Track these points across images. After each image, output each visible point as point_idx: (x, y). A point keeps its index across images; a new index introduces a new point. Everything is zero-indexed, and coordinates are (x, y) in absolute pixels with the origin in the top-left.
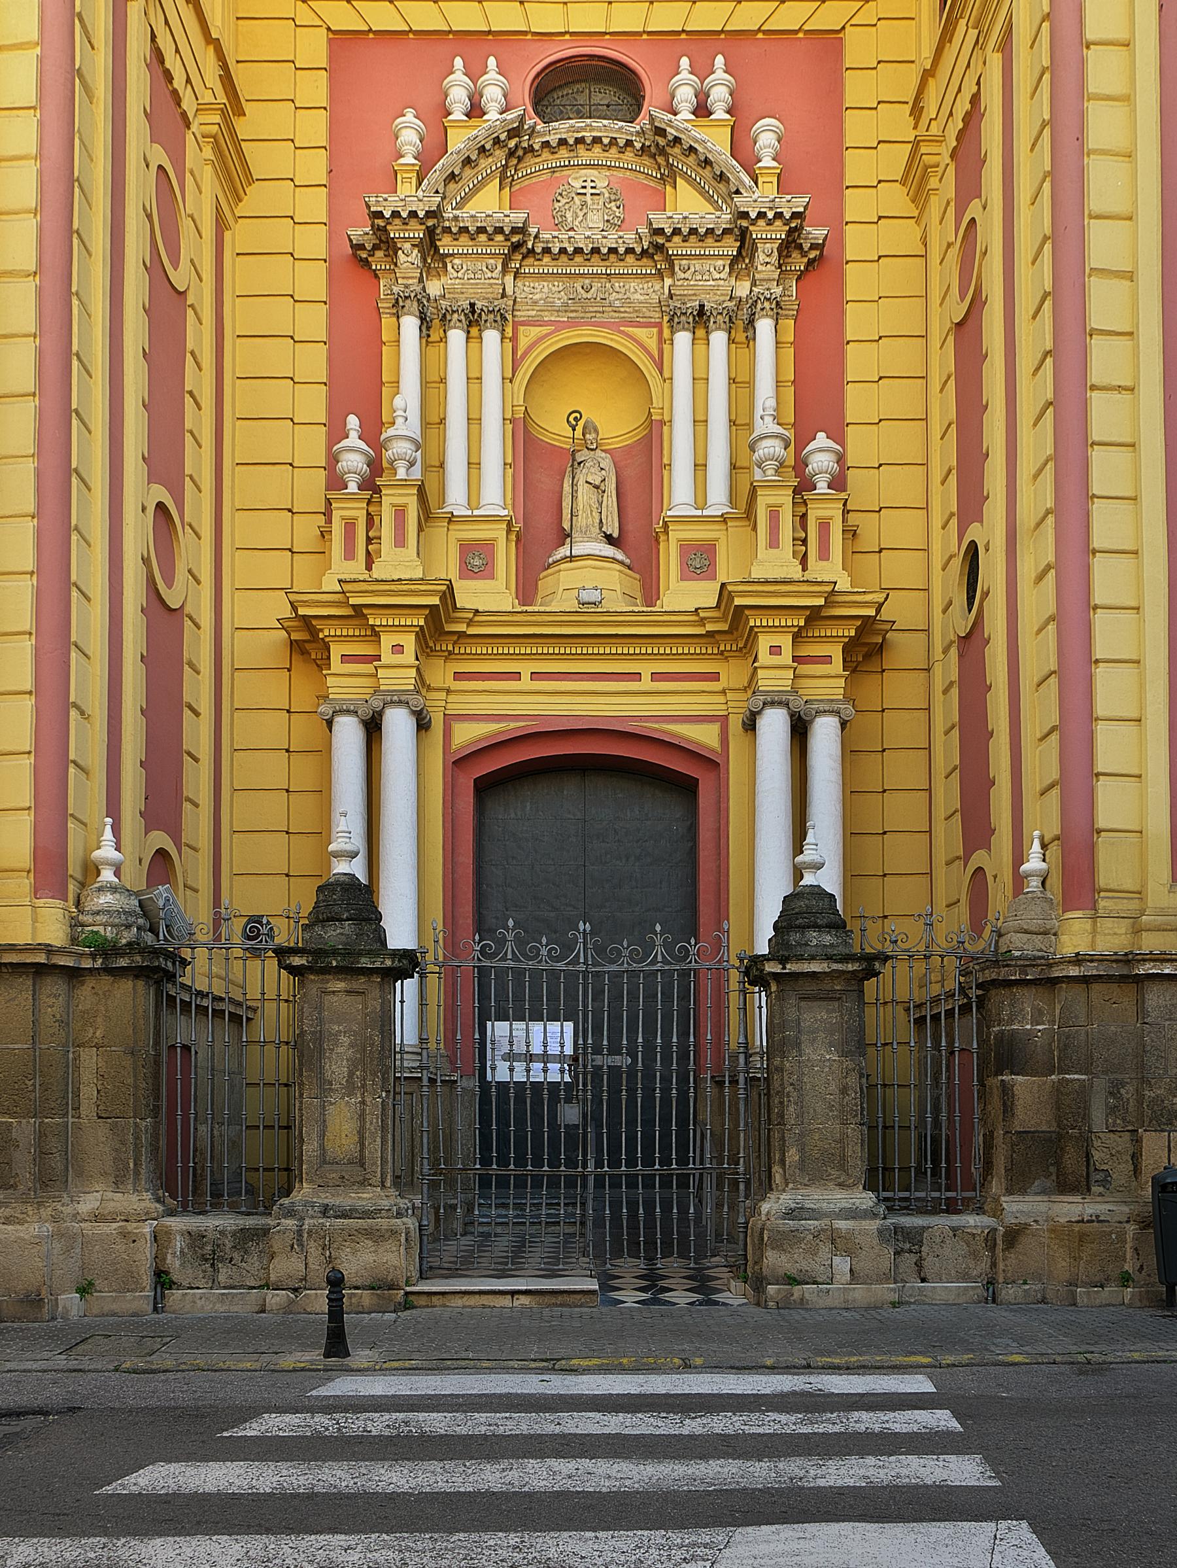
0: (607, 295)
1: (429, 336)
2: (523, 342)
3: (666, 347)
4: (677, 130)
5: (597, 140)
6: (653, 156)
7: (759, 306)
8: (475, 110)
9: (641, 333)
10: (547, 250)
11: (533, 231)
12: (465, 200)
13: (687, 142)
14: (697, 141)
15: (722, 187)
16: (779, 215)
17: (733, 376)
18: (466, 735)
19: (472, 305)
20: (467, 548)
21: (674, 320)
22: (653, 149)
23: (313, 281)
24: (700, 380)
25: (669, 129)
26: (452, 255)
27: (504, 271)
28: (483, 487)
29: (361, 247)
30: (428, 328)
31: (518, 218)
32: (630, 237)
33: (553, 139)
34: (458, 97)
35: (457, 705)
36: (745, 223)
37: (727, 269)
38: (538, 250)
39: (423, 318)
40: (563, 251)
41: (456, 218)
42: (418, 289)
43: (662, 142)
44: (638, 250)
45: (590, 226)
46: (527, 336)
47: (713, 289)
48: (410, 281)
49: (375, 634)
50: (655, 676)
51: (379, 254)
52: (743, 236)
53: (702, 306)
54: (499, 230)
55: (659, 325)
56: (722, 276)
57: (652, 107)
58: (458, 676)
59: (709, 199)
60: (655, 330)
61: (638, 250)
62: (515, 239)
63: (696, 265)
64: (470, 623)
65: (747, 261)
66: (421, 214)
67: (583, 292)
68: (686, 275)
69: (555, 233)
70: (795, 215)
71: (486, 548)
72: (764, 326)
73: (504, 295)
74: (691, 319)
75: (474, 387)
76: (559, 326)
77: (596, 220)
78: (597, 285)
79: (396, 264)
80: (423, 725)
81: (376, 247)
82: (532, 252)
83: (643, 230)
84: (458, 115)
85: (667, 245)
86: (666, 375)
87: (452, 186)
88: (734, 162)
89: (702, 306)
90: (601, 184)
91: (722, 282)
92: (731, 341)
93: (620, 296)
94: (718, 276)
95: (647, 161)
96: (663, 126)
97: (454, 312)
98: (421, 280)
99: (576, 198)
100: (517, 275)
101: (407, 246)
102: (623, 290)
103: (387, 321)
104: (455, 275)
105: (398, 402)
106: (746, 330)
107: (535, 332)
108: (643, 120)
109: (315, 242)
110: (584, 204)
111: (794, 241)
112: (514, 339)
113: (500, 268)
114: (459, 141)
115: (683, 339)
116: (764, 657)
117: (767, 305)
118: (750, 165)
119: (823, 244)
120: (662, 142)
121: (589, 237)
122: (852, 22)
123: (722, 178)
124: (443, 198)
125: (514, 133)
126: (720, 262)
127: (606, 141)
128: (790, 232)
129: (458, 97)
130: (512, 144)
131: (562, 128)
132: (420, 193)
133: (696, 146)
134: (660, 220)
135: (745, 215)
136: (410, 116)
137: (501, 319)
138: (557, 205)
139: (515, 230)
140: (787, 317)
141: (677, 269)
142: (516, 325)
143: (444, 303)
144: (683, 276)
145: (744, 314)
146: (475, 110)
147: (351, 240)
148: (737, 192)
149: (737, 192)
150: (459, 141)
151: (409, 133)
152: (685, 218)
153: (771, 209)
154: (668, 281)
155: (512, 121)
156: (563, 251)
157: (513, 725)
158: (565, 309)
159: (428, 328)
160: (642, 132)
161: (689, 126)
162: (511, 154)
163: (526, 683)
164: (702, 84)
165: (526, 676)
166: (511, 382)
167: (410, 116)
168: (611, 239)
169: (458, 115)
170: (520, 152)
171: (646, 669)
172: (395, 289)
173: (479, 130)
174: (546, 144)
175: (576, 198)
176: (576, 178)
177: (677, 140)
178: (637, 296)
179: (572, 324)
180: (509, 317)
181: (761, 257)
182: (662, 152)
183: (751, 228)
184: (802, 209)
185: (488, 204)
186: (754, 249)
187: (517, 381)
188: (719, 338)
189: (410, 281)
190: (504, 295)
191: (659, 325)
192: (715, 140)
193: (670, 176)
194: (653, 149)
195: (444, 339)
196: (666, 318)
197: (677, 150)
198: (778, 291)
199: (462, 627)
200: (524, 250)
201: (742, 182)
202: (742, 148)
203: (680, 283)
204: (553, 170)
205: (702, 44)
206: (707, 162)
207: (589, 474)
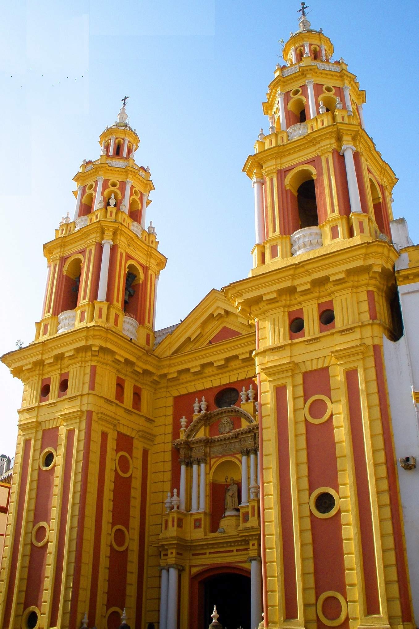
2: (212, 463)
18: (194, 570)
20: (196, 521)
23: (168, 456)
28: (201, 503)
33: (216, 413)
34: (196, 408)
35: (194, 562)
46: (213, 461)
49: (167, 550)
50: (237, 551)
58: (193, 555)
64: (191, 543)
71: (200, 520)
76: (220, 457)
77: (227, 430)
80: (181, 571)
84: (196, 413)
90: (229, 420)
100: (210, 447)
109: (169, 447)
115: (244, 458)
116: (251, 546)
129: (196, 408)
142: (211, 459)
146: (200, 410)
157: (204, 567)
163: (208, 555)
165: (208, 554)
169: (196, 413)
171: (234, 549)
174: (215, 415)
199: (190, 544)
207: (230, 493)
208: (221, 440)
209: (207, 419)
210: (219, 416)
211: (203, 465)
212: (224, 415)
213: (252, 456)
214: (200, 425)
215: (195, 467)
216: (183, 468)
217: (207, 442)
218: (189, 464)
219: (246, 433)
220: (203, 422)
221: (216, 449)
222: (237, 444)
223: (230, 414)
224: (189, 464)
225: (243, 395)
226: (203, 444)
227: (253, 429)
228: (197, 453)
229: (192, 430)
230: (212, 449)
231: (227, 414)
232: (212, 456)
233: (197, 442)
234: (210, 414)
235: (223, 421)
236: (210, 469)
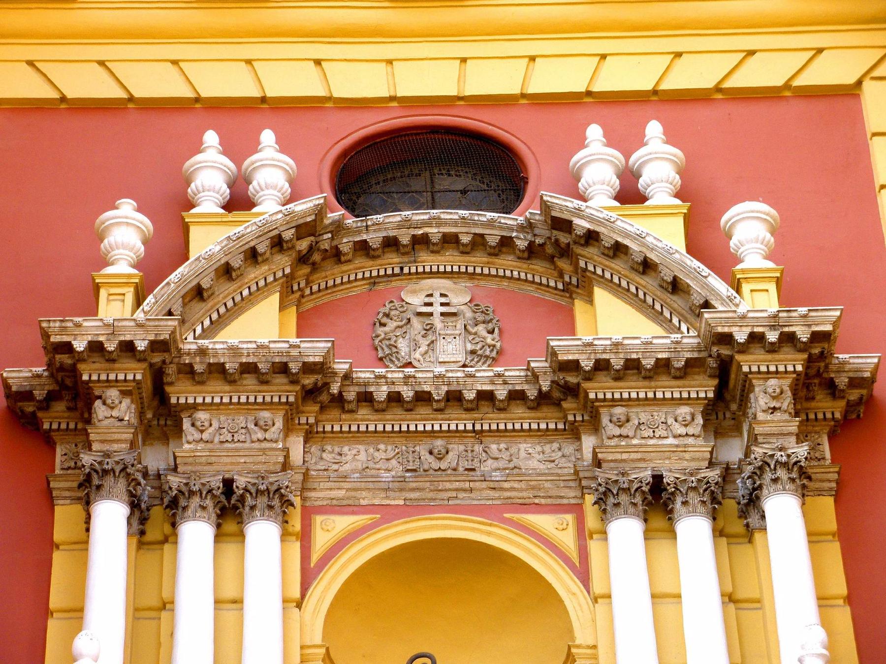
0: (476, 464)
1: (142, 533)
2: (322, 540)
3: (594, 546)
4: (591, 219)
5: (450, 240)
6: (551, 259)
7: (768, 476)
8: (239, 201)
9: (545, 522)
10: (366, 398)
11: (341, 366)
12: (217, 325)
13: (609, 237)
14: (627, 235)
15: (677, 301)
16: (788, 339)
17: (729, 589)
19: (228, 483)
21: (608, 500)
22: (549, 250)
24: (665, 599)
25: (577, 221)
26: (195, 407)
27: (288, 429)
29: (26, 395)
30: (143, 521)
31: (314, 349)
32: (515, 374)
33: (374, 238)
36: (725, 351)
37: (700, 420)
38: (351, 394)
39: (134, 505)
40: (395, 398)
41: (202, 352)
42: (129, 459)
43: (564, 239)
44: (532, 393)
45: (446, 360)
46: (328, 529)
47: (674, 450)
48: (116, 447)
51: (59, 407)
52: (724, 371)
53: (658, 479)
54: (283, 369)
55: (577, 509)
56: (691, 430)
57: (544, 194)
59: (657, 316)
60: (569, 518)
61: (532, 393)
62: (308, 381)
63: (642, 415)
65: (734, 407)
66: (141, 345)
67: (431, 459)
68: (624, 431)
69: (381, 371)
70: (817, 337)
72: (782, 510)
73: (286, 466)
74: (638, 499)
75: (229, 615)
76: (388, 514)
78: (456, 448)
79: (88, 421)
81: (52, 397)
82: (339, 400)
83: (539, 364)
85: (585, 385)
86: (597, 587)
87: (198, 308)
88: (696, 263)
89: (658, 479)
91: (691, 441)
92: (719, 533)
93: (501, 464)
94: (682, 431)
95: (539, 266)
96: (566, 216)
97: (192, 493)
98: (133, 445)
99: (415, 321)
100: (309, 436)
101: (113, 394)
102: (505, 455)
103: (65, 515)
104: (197, 436)
105: (81, 643)
106: (743, 514)
107: (342, 523)
108: (528, 210)
110: (429, 329)
111: (818, 374)
112: (305, 537)
113: (279, 424)
114: (209, 241)
115: (626, 531)
117: (782, 473)
118: (723, 263)
119: (872, 380)
120: (564, 239)
121: (440, 376)
122: (876, 73)
123: (676, 286)
124: (183, 322)
125: (305, 229)
126: (684, 411)
127: (465, 239)
128: (810, 360)
130: (303, 245)
131: (388, 222)
132: (139, 315)
133: (627, 242)
134: (565, 347)
135: (726, 339)
136: (127, 208)
137: (278, 502)
138: (380, 331)
139: (308, 368)
140: (820, 492)
141: (605, 420)
142: (308, 514)
143: (174, 481)
144: (617, 431)
145: (741, 486)
146: (239, 201)
147: (7, 387)
148: (707, 305)
149: (707, 305)
150: (209, 241)
151: (126, 231)
152: (617, 345)
153: (773, 327)
154: (588, 442)
155: (305, 214)
156: (395, 398)
158: (401, 484)
159: (143, 521)
160: (529, 226)
161: (614, 215)
162: (302, 259)
164: (627, 160)
166: (299, 606)
167: (127, 208)
168: (484, 376)
170: (316, 257)
172: (87, 459)
173: (246, 227)
174: (363, 247)
175: (415, 321)
176: (414, 292)
177: (591, 237)
178: (534, 464)
179: (411, 509)
180: (297, 501)
181: (760, 400)
182: (565, 252)
183: (738, 357)
184: (828, 328)
185: (261, 327)
186: (747, 388)
187: (310, 602)
188: (694, 530)
189: (116, 447)
190: (286, 466)
191: (577, 509)
192: (661, 232)
193: (580, 286)
194: (549, 250)
195: (171, 538)
196: (590, 499)
197: (592, 251)
198: (801, 451)
200: (324, 397)
201: (712, 290)
202: (705, 239)
203: (607, 442)
204: (373, 281)
205: (623, 110)
206: (647, 266)
208: (422, 398)
209: (303, 257)
210: (392, 261)
211: (262, 534)
212: (428, 261)
213: (694, 530)
214: (255, 274)
215: (196, 534)
216: (111, 516)
217: (314, 395)
218: (155, 516)
219: (663, 366)
220: (283, 263)
221: (357, 459)
222: (524, 447)
223: (477, 262)
224: (155, 516)
225: (597, 166)
226: (282, 391)
227: (756, 338)
228: (219, 440)
229: (198, 293)
230: (327, 456)
231: (450, 260)
232: (320, 495)
233: (249, 369)
234: (338, 228)
235: (416, 300)
236: (307, 579)
